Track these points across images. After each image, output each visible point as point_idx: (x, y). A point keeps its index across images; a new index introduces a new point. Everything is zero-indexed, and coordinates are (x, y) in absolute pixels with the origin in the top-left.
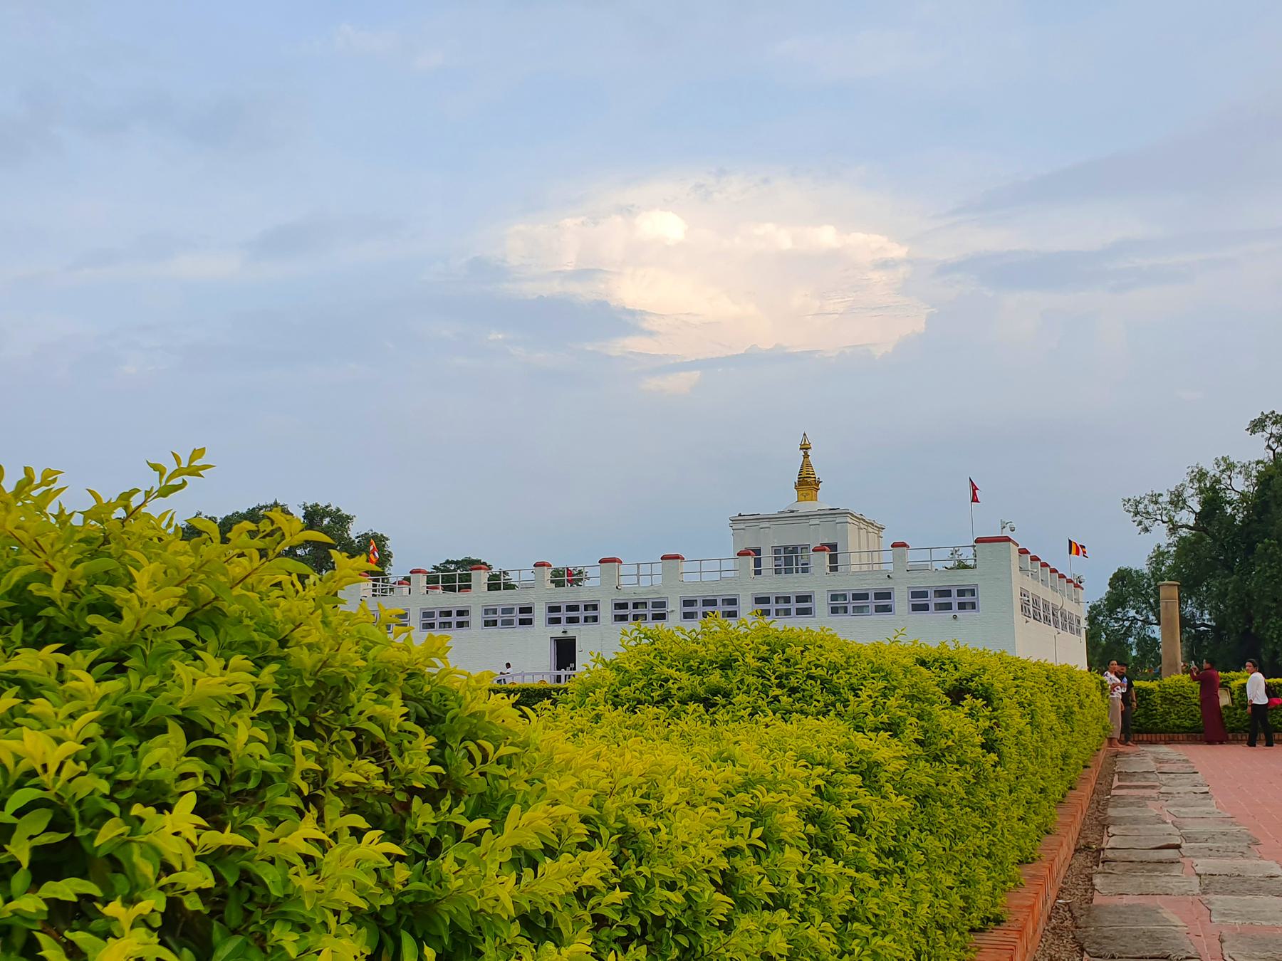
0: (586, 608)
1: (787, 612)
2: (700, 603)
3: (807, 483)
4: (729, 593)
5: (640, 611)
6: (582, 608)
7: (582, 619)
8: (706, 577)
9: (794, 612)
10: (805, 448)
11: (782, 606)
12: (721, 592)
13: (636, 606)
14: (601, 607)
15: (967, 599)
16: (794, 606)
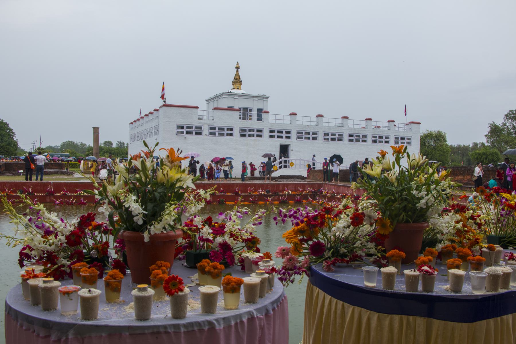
0: (228, 129)
1: (309, 138)
2: (276, 132)
4: (288, 129)
5: (252, 133)
6: (226, 129)
7: (225, 134)
8: (277, 122)
9: (311, 138)
10: (238, 68)
11: (307, 136)
12: (284, 128)
13: (250, 130)
14: (234, 130)
15: (364, 139)
16: (311, 136)
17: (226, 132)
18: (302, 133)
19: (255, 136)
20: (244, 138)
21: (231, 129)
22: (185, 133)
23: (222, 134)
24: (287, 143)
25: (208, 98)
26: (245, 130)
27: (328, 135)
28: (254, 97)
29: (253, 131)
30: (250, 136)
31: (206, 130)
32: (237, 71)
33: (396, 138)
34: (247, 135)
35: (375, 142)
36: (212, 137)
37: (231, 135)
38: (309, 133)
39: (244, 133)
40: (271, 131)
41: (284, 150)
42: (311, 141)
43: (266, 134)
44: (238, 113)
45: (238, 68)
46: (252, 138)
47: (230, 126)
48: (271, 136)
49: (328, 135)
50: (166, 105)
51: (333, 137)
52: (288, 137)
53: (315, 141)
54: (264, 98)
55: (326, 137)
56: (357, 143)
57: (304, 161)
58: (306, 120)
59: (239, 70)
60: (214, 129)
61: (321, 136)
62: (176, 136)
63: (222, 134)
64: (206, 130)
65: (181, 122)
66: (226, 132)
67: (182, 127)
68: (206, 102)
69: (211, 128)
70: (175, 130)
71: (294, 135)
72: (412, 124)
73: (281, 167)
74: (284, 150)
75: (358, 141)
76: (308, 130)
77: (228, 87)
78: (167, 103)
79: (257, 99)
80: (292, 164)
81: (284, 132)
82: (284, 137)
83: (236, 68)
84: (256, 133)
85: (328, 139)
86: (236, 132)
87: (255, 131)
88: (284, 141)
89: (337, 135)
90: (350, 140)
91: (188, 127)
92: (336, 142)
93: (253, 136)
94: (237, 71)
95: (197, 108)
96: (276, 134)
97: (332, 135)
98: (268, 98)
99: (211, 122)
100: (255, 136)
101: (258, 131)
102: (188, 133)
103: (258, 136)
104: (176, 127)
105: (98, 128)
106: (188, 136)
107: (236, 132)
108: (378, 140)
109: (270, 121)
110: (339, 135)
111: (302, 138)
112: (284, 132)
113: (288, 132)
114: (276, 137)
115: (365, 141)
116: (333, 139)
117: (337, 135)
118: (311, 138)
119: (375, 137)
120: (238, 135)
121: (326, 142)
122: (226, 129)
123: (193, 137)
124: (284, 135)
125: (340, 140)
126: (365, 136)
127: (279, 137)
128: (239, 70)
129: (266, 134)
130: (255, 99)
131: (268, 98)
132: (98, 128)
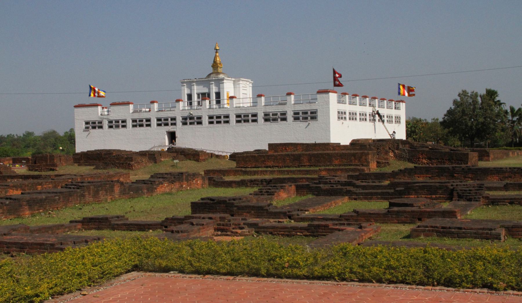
11: (192, 121)
23: (117, 127)
31: (106, 124)
41: (172, 136)
43: (154, 122)
46: (142, 128)
47: (124, 118)
51: (219, 120)
52: (175, 124)
53: (199, 126)
61: (205, 120)
64: (106, 124)
65: (88, 119)
70: (84, 126)
74: (172, 136)
86: (129, 123)
88: (171, 128)
92: (223, 124)
104: (84, 123)
107: (129, 123)
120: (131, 126)
121: (211, 125)
123: (97, 130)
129: (154, 122)
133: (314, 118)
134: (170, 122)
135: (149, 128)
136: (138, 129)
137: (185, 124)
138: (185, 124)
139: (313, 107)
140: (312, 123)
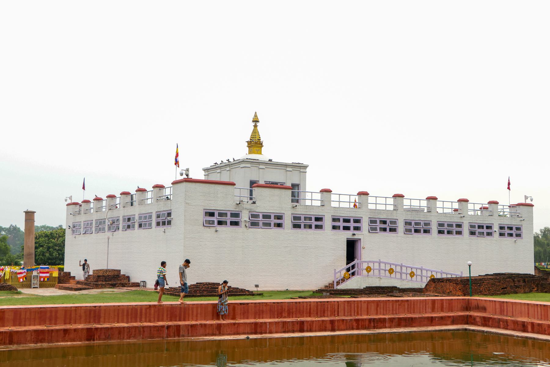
1: (385, 230)
2: (341, 220)
3: (255, 144)
6: (272, 217)
8: (342, 205)
9: (388, 229)
10: (256, 121)
11: (383, 226)
13: (305, 218)
15: (459, 229)
17: (273, 221)
18: (375, 222)
19: (313, 227)
20: (298, 230)
21: (279, 217)
22: (216, 223)
24: (356, 237)
25: (208, 166)
26: (299, 218)
27: (410, 224)
28: (286, 165)
29: (310, 219)
30: (305, 226)
32: (255, 126)
33: (501, 228)
34: (302, 226)
35: (472, 233)
36: (254, 230)
37: (279, 225)
38: (384, 222)
39: (297, 222)
40: (334, 220)
41: (352, 248)
42: (388, 234)
43: (328, 223)
44: (289, 192)
45: (256, 121)
48: (334, 228)
49: (410, 224)
50: (188, 180)
52: (357, 228)
54: (301, 168)
55: (409, 227)
56: (450, 236)
57: (385, 263)
58: (380, 203)
59: (258, 124)
60: (257, 216)
61: (401, 227)
62: (203, 228)
63: (269, 225)
66: (273, 221)
67: (212, 214)
68: (203, 173)
69: (253, 216)
70: (201, 217)
71: (365, 225)
72: (521, 207)
73: (353, 274)
74: (352, 248)
75: (449, 232)
76: (383, 217)
77: (242, 152)
78: (190, 177)
79: (291, 169)
80: (369, 269)
81: (352, 221)
82: (352, 228)
83: (253, 121)
84: (314, 223)
85: (410, 231)
86: (287, 221)
87: (313, 219)
89: (422, 223)
90: (440, 232)
91: (220, 215)
93: (310, 227)
94: (255, 126)
95: (233, 184)
96: (341, 224)
97: (416, 224)
98: (306, 167)
99: (253, 207)
100: (313, 227)
101: (318, 219)
102: (220, 223)
103: (317, 227)
104: (202, 213)
105: (34, 212)
106: (219, 228)
107: (287, 221)
108: (478, 231)
109: (334, 204)
110: (426, 224)
111: (375, 229)
112: (352, 221)
113: (357, 221)
114: (341, 228)
115: (459, 233)
116: (417, 231)
117: (422, 223)
118: (388, 229)
119: (472, 226)
122: (272, 217)
123: (226, 231)
124: (352, 225)
125: (426, 231)
126: (395, 223)
127: (346, 228)
128: (258, 124)
129: (328, 223)
130: (288, 169)
131: (306, 167)
132: (34, 212)
133: (519, 235)
134: (352, 225)
135: (319, 231)
136: (302, 233)
137: (373, 230)
138: (373, 230)
139: (515, 223)
140: (518, 239)
